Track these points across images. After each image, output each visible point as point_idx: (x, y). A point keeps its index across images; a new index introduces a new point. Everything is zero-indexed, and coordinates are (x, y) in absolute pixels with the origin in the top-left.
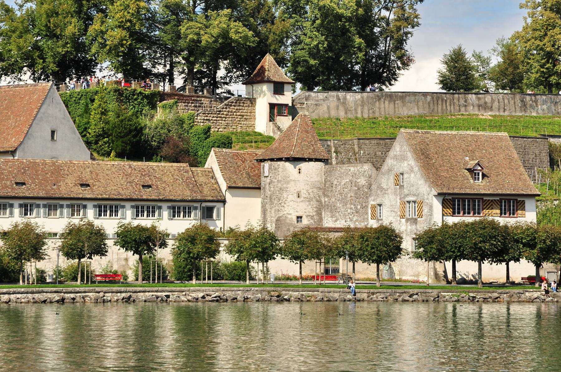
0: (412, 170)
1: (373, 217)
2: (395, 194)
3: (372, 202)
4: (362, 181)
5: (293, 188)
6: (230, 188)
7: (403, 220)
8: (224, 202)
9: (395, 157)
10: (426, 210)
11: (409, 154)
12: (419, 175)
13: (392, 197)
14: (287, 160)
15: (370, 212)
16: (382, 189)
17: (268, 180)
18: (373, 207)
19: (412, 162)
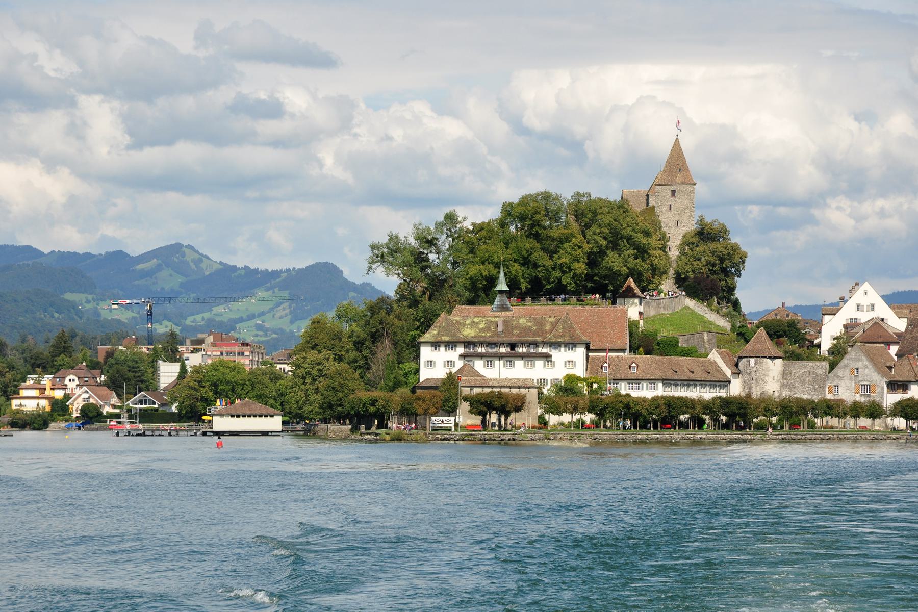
0: (866, 367)
1: (830, 392)
2: (851, 379)
3: (829, 384)
4: (820, 372)
5: (771, 374)
6: (733, 373)
7: (858, 395)
8: (730, 382)
9: (851, 359)
10: (878, 390)
11: (864, 358)
12: (872, 370)
13: (848, 382)
14: (770, 358)
15: (827, 390)
16: (838, 377)
17: (754, 369)
18: (829, 387)
19: (867, 363)
